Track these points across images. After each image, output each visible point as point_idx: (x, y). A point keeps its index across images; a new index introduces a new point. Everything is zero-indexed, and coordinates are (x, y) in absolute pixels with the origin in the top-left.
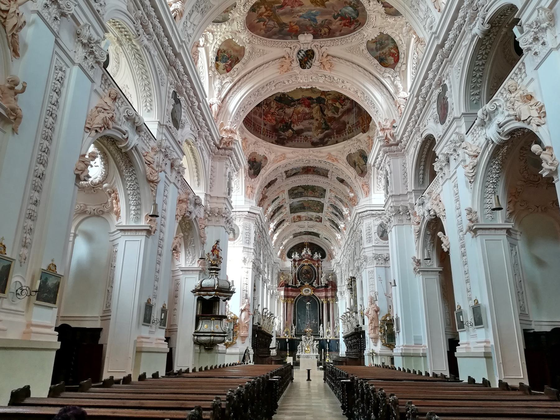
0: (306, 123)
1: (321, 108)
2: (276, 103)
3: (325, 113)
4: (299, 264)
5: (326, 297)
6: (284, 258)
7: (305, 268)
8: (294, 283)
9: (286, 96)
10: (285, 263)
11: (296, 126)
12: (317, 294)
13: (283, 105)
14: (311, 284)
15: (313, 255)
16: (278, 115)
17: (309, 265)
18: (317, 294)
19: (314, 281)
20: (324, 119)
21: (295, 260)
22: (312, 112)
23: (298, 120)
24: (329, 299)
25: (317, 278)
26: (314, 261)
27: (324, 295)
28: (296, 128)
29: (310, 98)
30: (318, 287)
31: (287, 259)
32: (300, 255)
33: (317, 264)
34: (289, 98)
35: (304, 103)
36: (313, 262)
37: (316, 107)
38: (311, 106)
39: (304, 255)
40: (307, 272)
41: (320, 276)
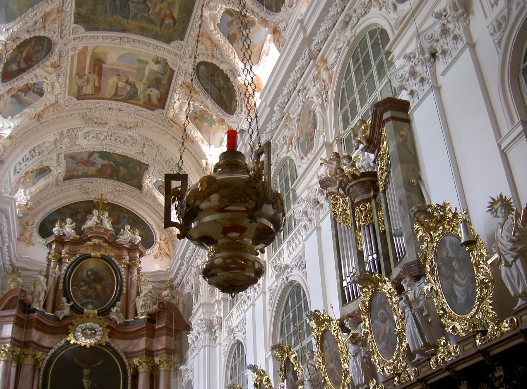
4: (72, 254)
5: (150, 353)
6: (27, 234)
7: (91, 264)
8: (50, 308)
10: (31, 249)
12: (120, 345)
14: (105, 313)
15: (117, 232)
17: (103, 257)
18: (120, 345)
19: (114, 305)
21: (61, 241)
24: (156, 360)
25: (122, 298)
26: (119, 247)
27: (142, 344)
30: (126, 324)
31: (37, 238)
32: (78, 230)
33: (128, 258)
36: (116, 252)
39: (90, 228)
40: (97, 277)
41: (134, 292)
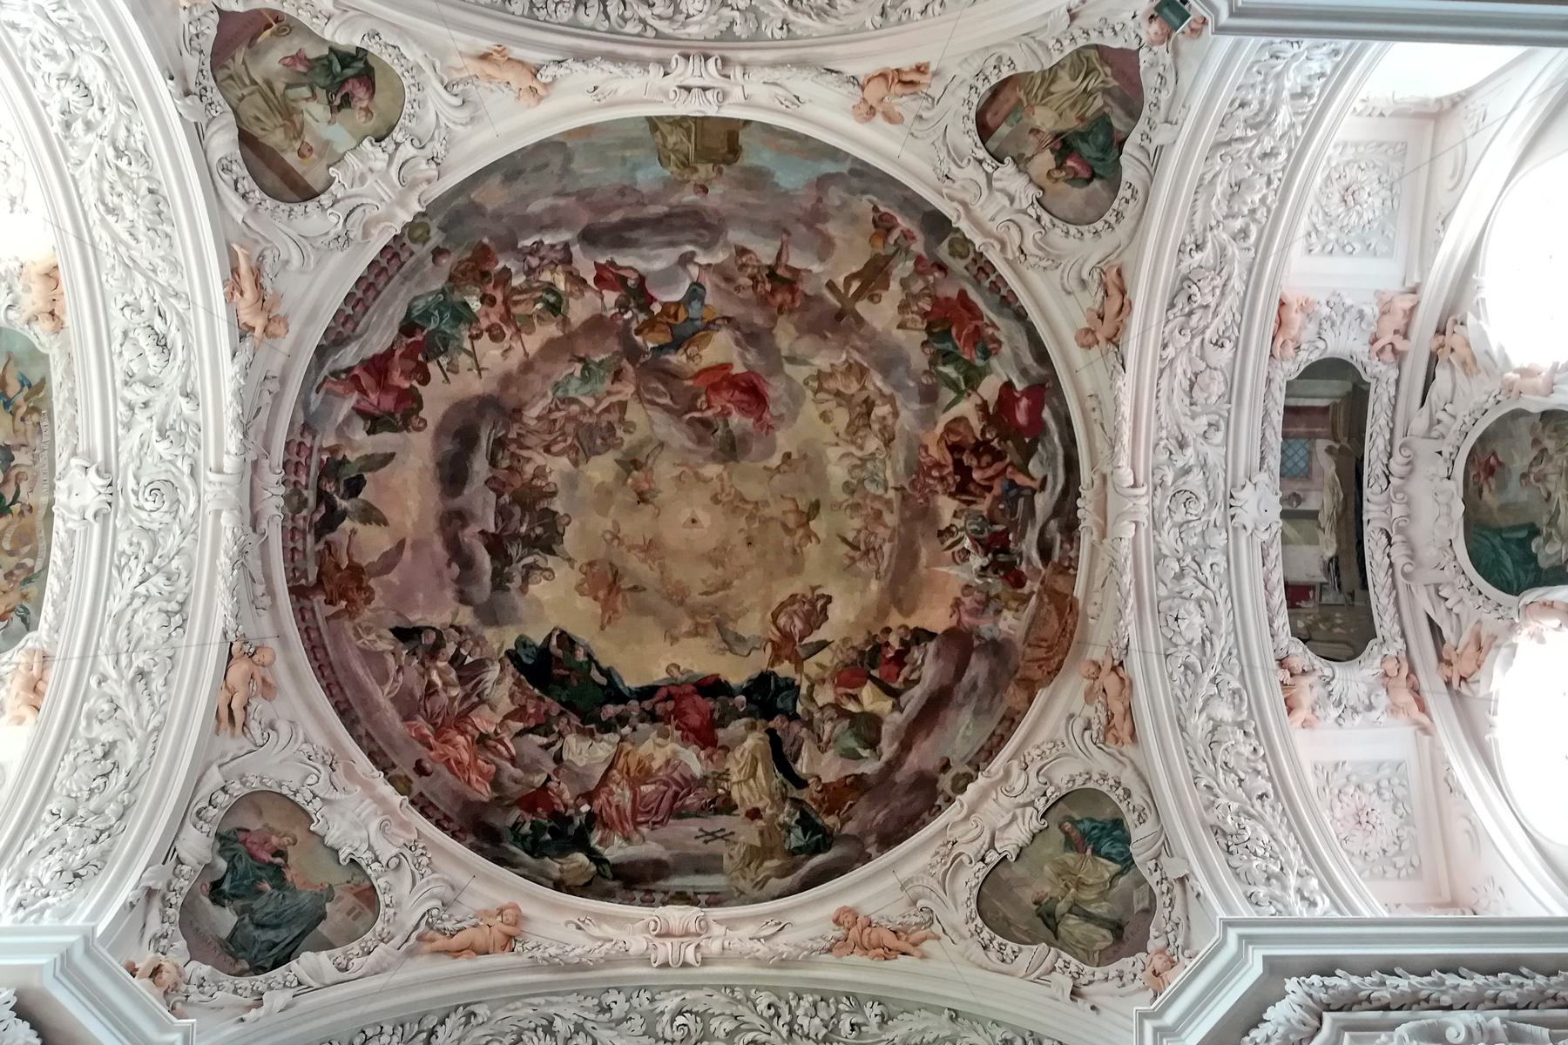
0: (686, 833)
1: (775, 741)
2: (518, 683)
3: (802, 767)
9: (580, 656)
11: (617, 841)
13: (556, 708)
16: (513, 760)
20: (797, 802)
22: (723, 776)
23: (635, 812)
28: (616, 850)
29: (713, 687)
34: (595, 674)
35: (679, 713)
37: (750, 742)
38: (720, 733)
